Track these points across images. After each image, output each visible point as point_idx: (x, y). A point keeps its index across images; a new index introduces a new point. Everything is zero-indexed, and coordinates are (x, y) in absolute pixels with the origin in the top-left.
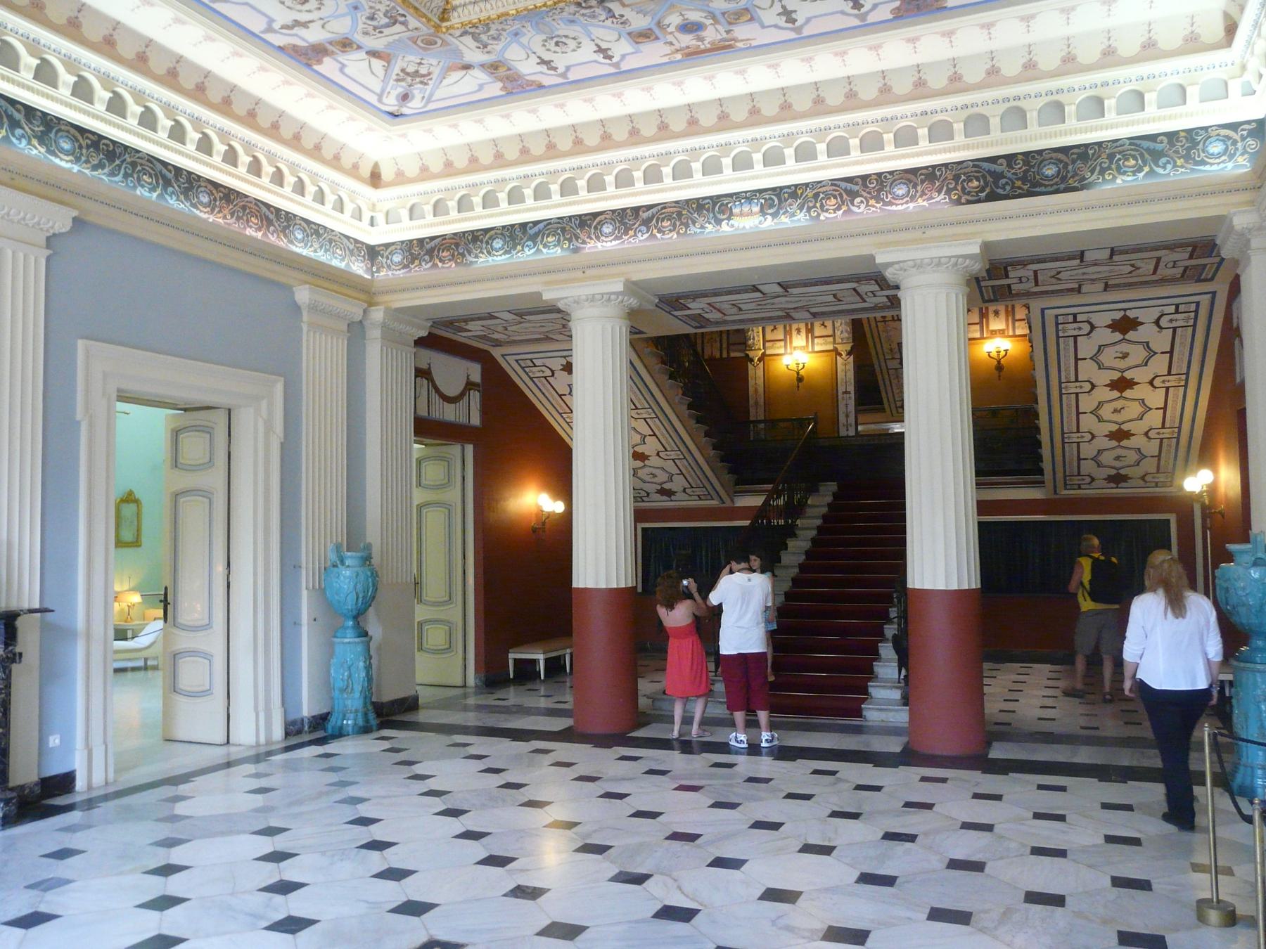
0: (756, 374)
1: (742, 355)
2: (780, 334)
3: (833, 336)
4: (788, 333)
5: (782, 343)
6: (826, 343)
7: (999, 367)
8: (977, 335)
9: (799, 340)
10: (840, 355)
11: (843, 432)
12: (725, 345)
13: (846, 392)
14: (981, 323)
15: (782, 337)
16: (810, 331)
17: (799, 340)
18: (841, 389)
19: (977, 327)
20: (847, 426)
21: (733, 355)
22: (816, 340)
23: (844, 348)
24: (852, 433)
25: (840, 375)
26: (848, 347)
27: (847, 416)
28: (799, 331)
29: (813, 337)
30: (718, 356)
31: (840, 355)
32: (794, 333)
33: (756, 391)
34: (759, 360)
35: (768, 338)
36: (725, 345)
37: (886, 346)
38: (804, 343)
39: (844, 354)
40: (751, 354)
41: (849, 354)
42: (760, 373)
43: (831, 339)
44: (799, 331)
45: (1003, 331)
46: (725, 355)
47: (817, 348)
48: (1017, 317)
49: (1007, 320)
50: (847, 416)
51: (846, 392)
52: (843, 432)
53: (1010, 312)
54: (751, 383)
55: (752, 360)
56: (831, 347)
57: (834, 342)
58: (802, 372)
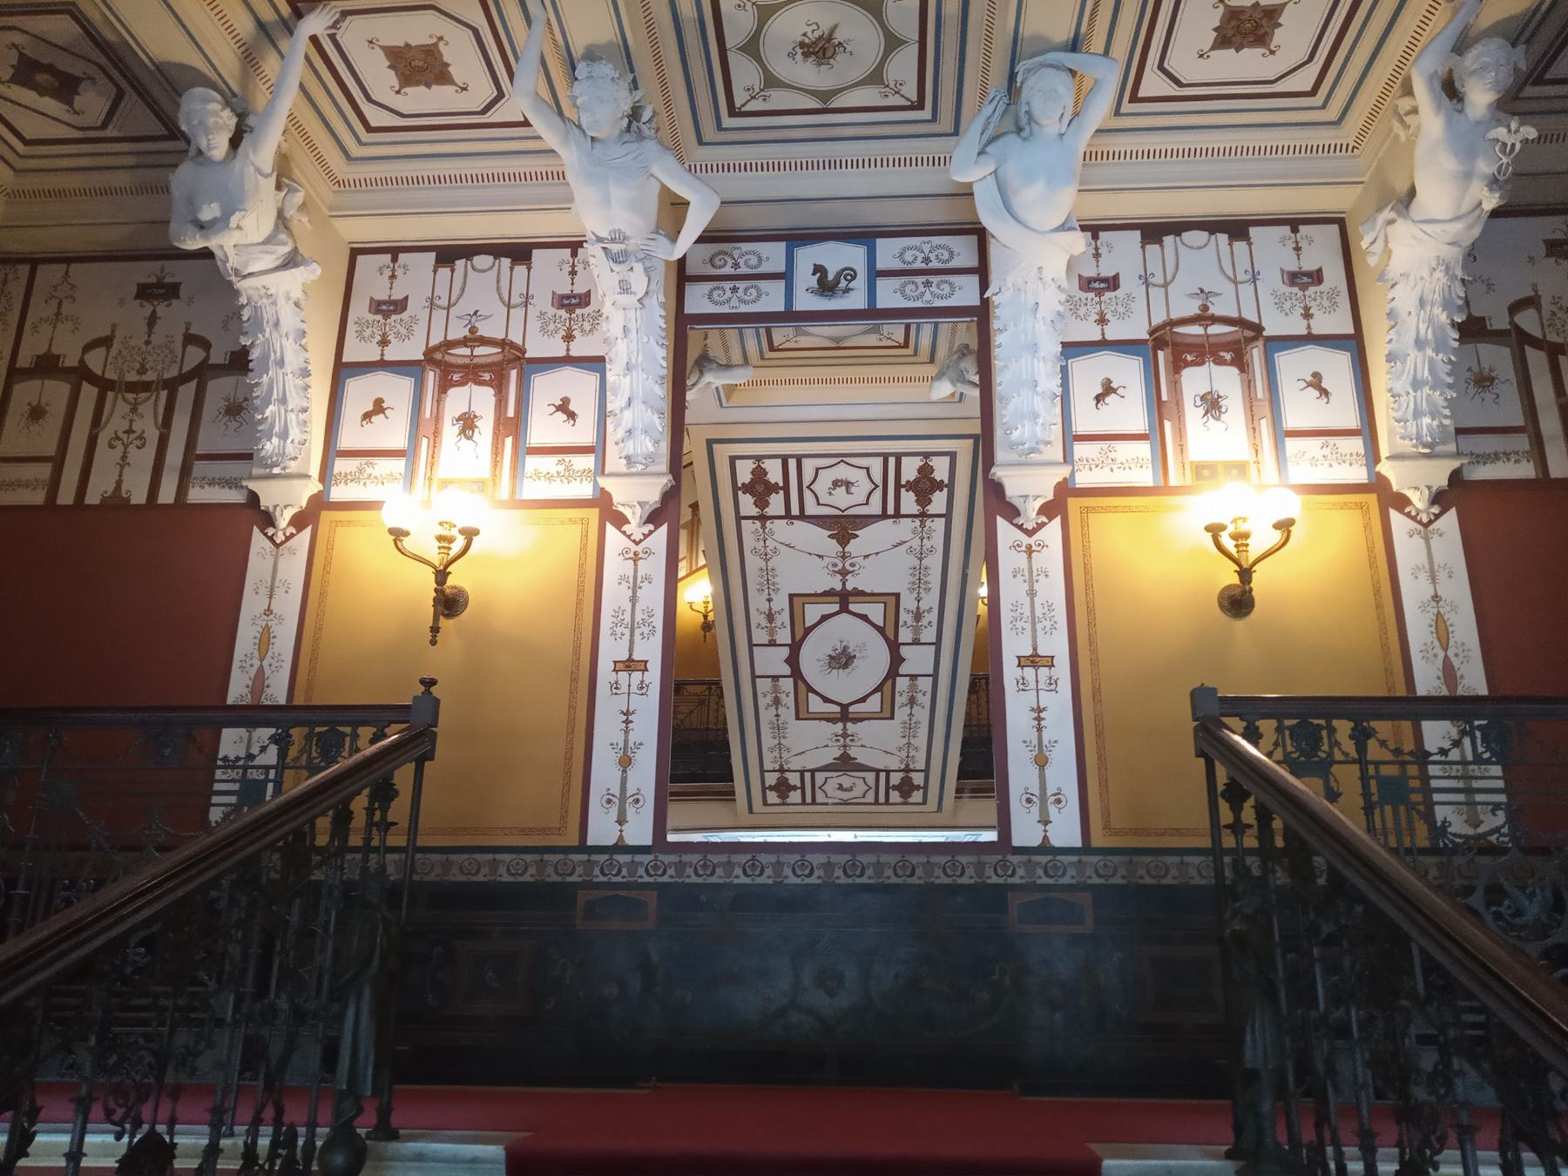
0: (274, 578)
1: (235, 497)
2: (392, 431)
3: (597, 449)
4: (423, 426)
5: (399, 465)
6: (569, 475)
7: (1238, 602)
8: (1145, 477)
9: (465, 457)
10: (620, 521)
11: (602, 830)
12: (175, 456)
13: (630, 665)
14: (1154, 435)
15: (399, 441)
16: (512, 425)
17: (465, 457)
18: (611, 650)
19: (1143, 449)
20: (622, 802)
21: (197, 495)
22: (532, 463)
23: (636, 493)
24: (639, 831)
25: (614, 596)
26: (652, 491)
27: (626, 762)
28: (467, 423)
29: (524, 450)
30: (139, 497)
31: (620, 521)
32: (450, 431)
33: (265, 640)
34: (299, 522)
35: (346, 441)
36: (175, 456)
37: (758, 602)
38: (483, 468)
39: (634, 516)
40: (269, 493)
41: (654, 518)
42: (293, 568)
43: (587, 462)
44: (467, 423)
45: (1241, 468)
46: (167, 495)
47: (534, 490)
48: (1291, 421)
49: (1254, 430)
50: (626, 762)
51: (630, 665)
52: (602, 830)
53: (1266, 402)
54: (252, 604)
55: (268, 520)
56: (585, 490)
57: (601, 469)
58: (458, 578)
